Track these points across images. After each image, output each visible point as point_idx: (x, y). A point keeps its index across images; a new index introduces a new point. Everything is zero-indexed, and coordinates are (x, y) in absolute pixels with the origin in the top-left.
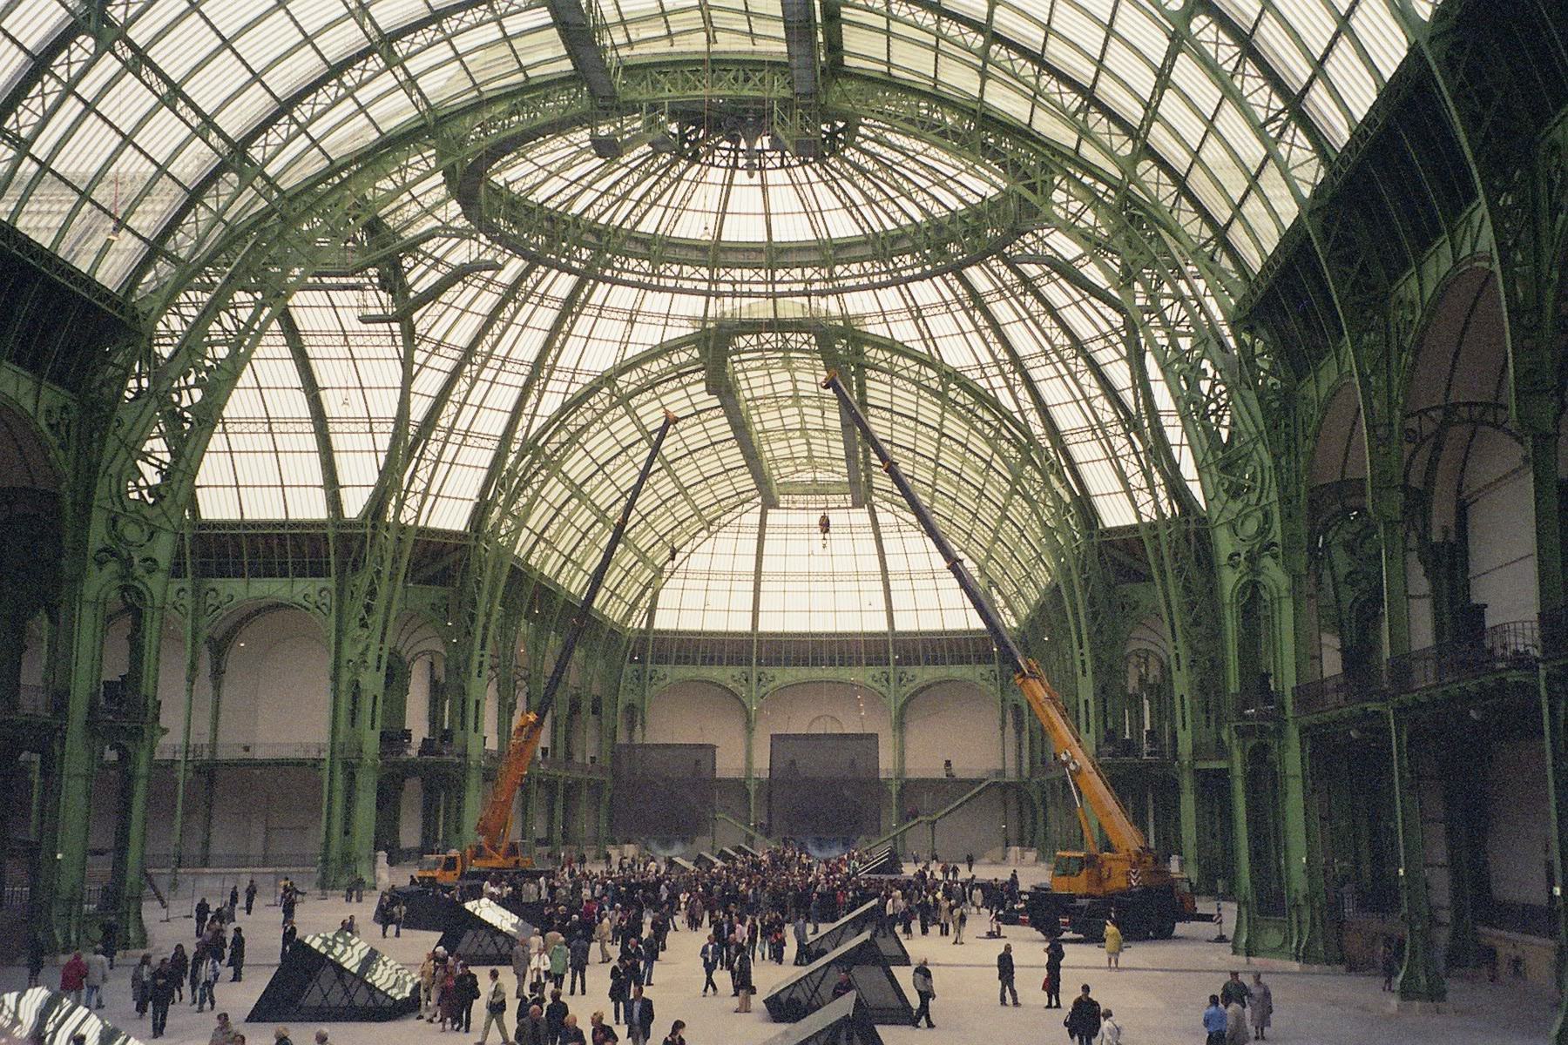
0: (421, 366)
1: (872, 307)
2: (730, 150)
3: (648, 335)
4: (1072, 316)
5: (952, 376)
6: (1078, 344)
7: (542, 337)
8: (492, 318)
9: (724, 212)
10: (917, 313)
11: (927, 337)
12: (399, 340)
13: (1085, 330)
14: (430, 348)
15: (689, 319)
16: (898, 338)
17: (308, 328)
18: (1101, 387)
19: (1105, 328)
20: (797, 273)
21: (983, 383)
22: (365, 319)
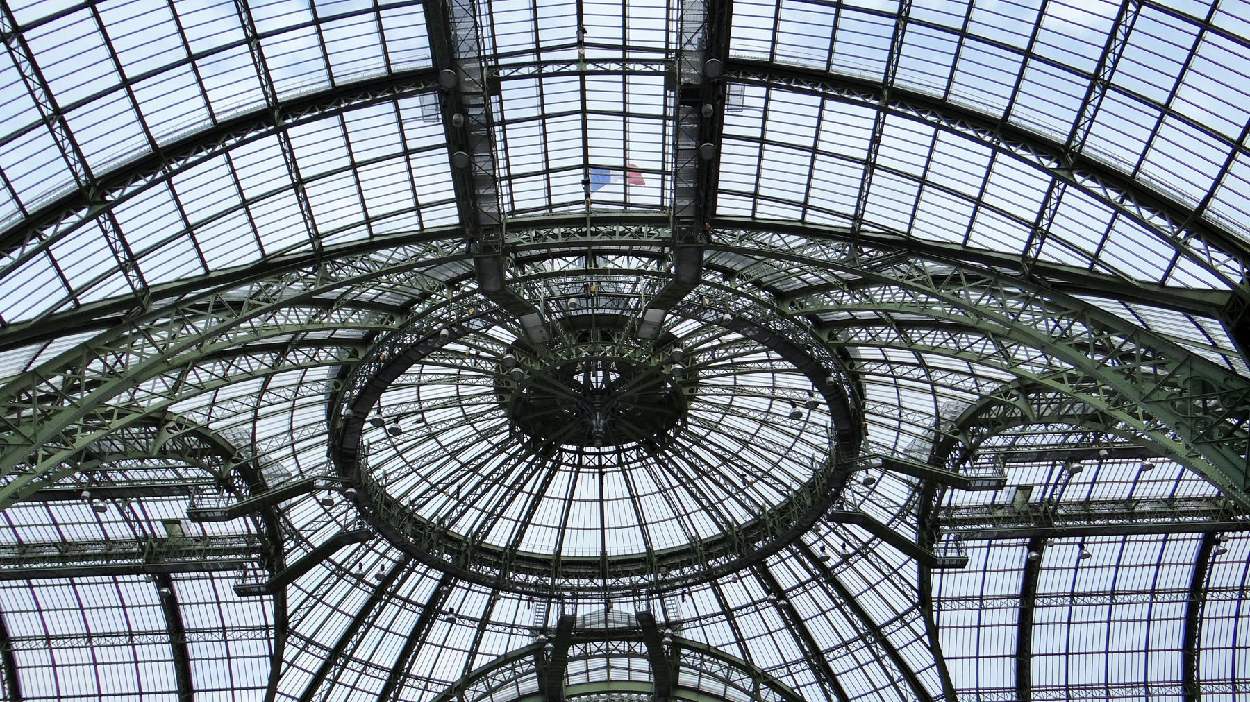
0: (291, 664)
1: (692, 608)
2: (575, 452)
3: (494, 645)
4: (869, 603)
5: (761, 677)
6: (874, 629)
7: (400, 643)
8: (358, 620)
9: (564, 528)
10: (728, 613)
11: (740, 640)
12: (272, 633)
13: (880, 616)
14: (301, 644)
15: (530, 629)
16: (712, 644)
17: (193, 626)
18: (901, 671)
19: (902, 605)
20: (626, 580)
21: (787, 682)
22: (242, 591)
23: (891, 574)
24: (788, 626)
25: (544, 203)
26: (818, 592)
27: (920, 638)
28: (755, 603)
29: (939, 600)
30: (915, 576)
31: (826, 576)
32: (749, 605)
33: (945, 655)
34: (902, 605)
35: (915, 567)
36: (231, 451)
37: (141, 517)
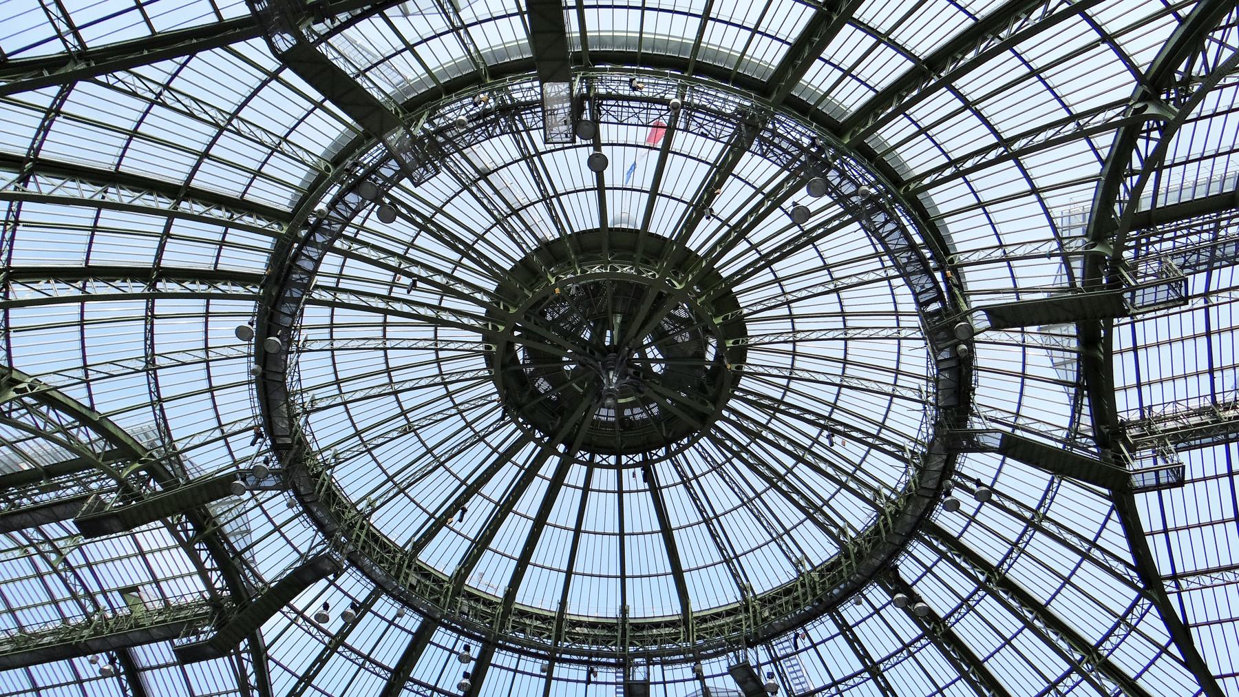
4: (1067, 609)
23: (1088, 551)
24: (963, 675)
25: (560, 190)
26: (989, 606)
27: (1164, 650)
28: (906, 646)
29: (1175, 577)
30: (1124, 543)
31: (995, 581)
32: (900, 651)
33: (1214, 671)
34: (1121, 596)
35: (1119, 529)
36: (139, 451)
37: (95, 588)
